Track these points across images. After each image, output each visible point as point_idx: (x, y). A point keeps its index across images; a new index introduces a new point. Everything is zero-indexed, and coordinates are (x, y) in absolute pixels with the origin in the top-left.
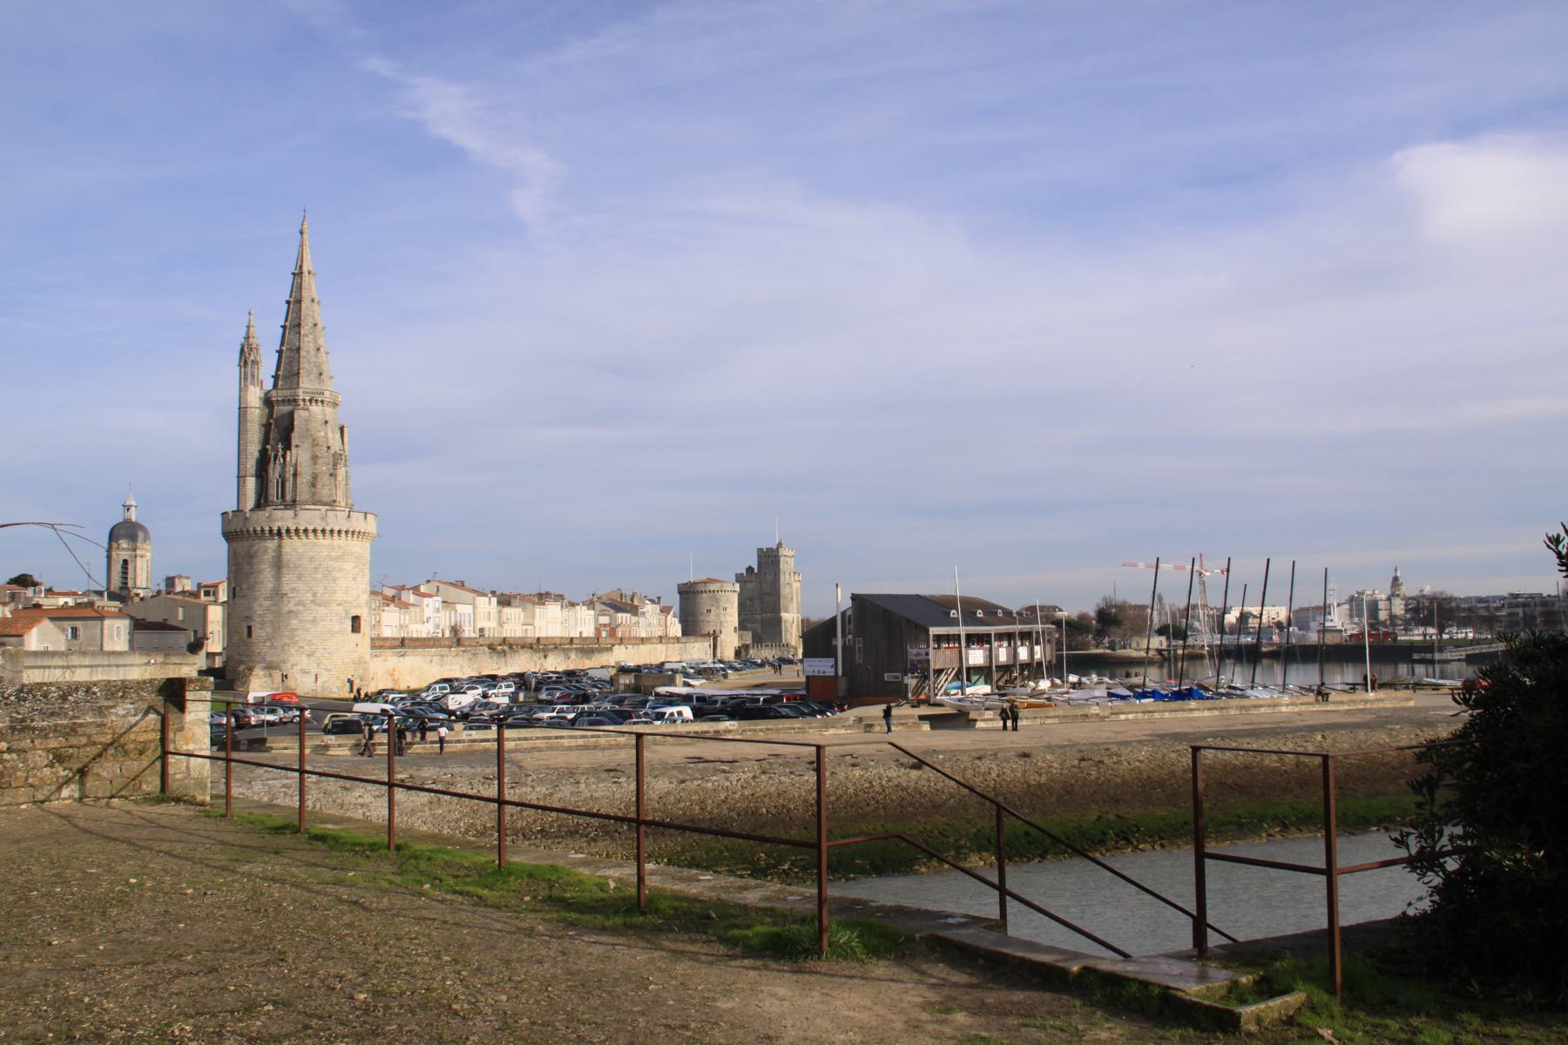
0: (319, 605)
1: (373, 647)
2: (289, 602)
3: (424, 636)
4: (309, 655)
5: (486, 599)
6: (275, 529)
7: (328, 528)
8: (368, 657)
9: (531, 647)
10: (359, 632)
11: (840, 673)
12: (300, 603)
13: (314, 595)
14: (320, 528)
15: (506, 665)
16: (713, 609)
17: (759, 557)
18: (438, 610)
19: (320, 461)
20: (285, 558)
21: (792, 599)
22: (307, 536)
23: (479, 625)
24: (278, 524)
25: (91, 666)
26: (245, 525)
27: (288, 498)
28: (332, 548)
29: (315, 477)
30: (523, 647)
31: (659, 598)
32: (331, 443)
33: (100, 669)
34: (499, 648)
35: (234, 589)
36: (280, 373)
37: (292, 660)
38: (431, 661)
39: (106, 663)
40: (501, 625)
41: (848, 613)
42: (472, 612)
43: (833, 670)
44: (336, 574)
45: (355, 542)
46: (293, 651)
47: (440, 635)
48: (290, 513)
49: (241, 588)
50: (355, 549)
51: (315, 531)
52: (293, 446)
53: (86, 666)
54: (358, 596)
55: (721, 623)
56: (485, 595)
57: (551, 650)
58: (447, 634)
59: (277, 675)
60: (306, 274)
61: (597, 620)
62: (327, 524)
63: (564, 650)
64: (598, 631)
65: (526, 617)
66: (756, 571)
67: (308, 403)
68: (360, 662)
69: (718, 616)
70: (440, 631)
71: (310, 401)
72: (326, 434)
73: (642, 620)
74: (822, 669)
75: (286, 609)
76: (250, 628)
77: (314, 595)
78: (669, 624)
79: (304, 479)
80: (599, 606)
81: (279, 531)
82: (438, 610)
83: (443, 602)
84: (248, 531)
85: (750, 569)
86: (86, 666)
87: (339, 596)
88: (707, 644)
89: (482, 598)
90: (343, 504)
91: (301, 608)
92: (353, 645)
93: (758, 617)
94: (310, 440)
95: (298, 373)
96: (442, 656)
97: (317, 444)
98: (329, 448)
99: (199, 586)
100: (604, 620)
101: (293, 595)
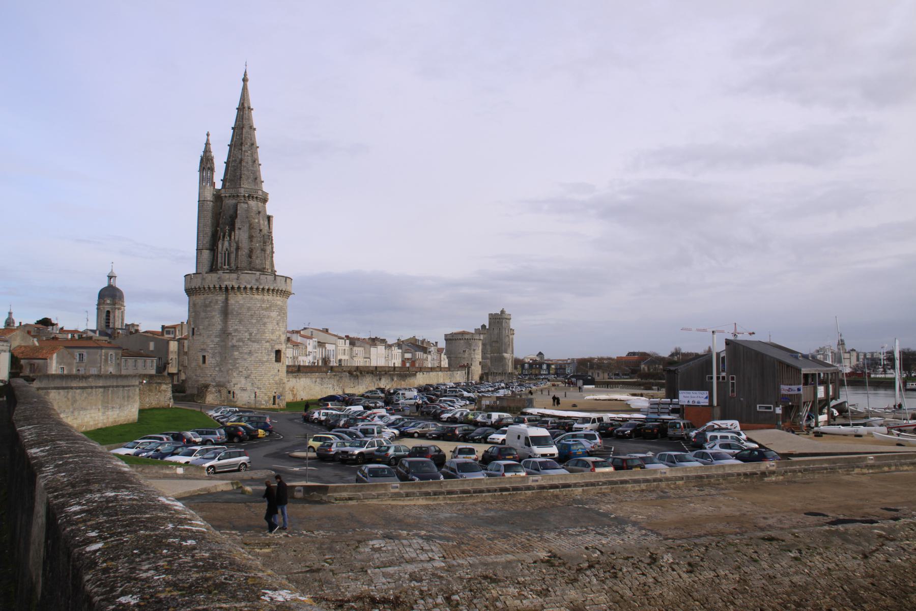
0: (254, 342)
1: (288, 372)
2: (233, 339)
3: (307, 364)
4: (246, 377)
5: (343, 341)
6: (223, 286)
7: (261, 287)
8: (285, 380)
9: (372, 373)
10: (280, 361)
11: (715, 403)
12: (240, 340)
13: (251, 334)
14: (255, 287)
15: (358, 384)
16: (467, 350)
17: (490, 319)
18: (315, 348)
19: (255, 240)
20: (230, 308)
21: (509, 344)
22: (246, 292)
23: (339, 358)
24: (226, 283)
25: (104, 387)
26: (201, 284)
27: (233, 265)
28: (263, 301)
29: (251, 251)
30: (368, 373)
31: (436, 343)
32: (262, 227)
33: (111, 389)
34: (355, 373)
35: (193, 329)
36: (228, 177)
37: (234, 381)
38: (316, 382)
39: (115, 384)
40: (352, 357)
41: (722, 355)
42: (334, 349)
43: (707, 400)
44: (266, 320)
45: (279, 298)
46: (235, 374)
47: (316, 364)
48: (234, 276)
49: (198, 329)
50: (279, 303)
51: (251, 288)
52: (236, 229)
53: (100, 387)
54: (280, 336)
55: (472, 359)
56: (342, 338)
57: (383, 375)
58: (320, 364)
59: (224, 392)
60: (247, 109)
61: (403, 356)
62: (260, 284)
63: (390, 375)
64: (404, 362)
65: (365, 353)
66: (487, 327)
67: (247, 199)
68: (280, 383)
69: (470, 354)
70: (316, 361)
71: (249, 197)
72: (259, 221)
73: (429, 357)
74: (696, 400)
75: (230, 344)
76: (204, 357)
77: (251, 334)
78: (442, 359)
79: (244, 252)
80: (404, 347)
81: (226, 288)
82: (315, 348)
83: (319, 342)
84: (204, 288)
85: (484, 326)
86: (100, 387)
87: (268, 336)
88: (464, 372)
89: (341, 340)
90: (270, 271)
91: (241, 344)
92: (276, 371)
93: (489, 356)
94: (248, 225)
95: (241, 177)
96: (322, 378)
97: (253, 228)
98: (261, 230)
99: (163, 327)
100: (408, 356)
101: (236, 334)
